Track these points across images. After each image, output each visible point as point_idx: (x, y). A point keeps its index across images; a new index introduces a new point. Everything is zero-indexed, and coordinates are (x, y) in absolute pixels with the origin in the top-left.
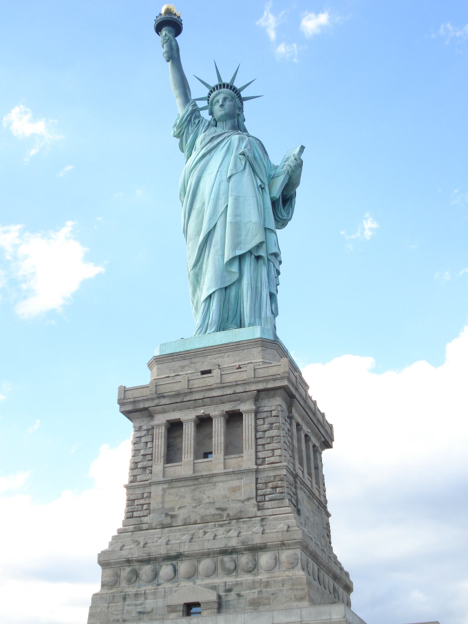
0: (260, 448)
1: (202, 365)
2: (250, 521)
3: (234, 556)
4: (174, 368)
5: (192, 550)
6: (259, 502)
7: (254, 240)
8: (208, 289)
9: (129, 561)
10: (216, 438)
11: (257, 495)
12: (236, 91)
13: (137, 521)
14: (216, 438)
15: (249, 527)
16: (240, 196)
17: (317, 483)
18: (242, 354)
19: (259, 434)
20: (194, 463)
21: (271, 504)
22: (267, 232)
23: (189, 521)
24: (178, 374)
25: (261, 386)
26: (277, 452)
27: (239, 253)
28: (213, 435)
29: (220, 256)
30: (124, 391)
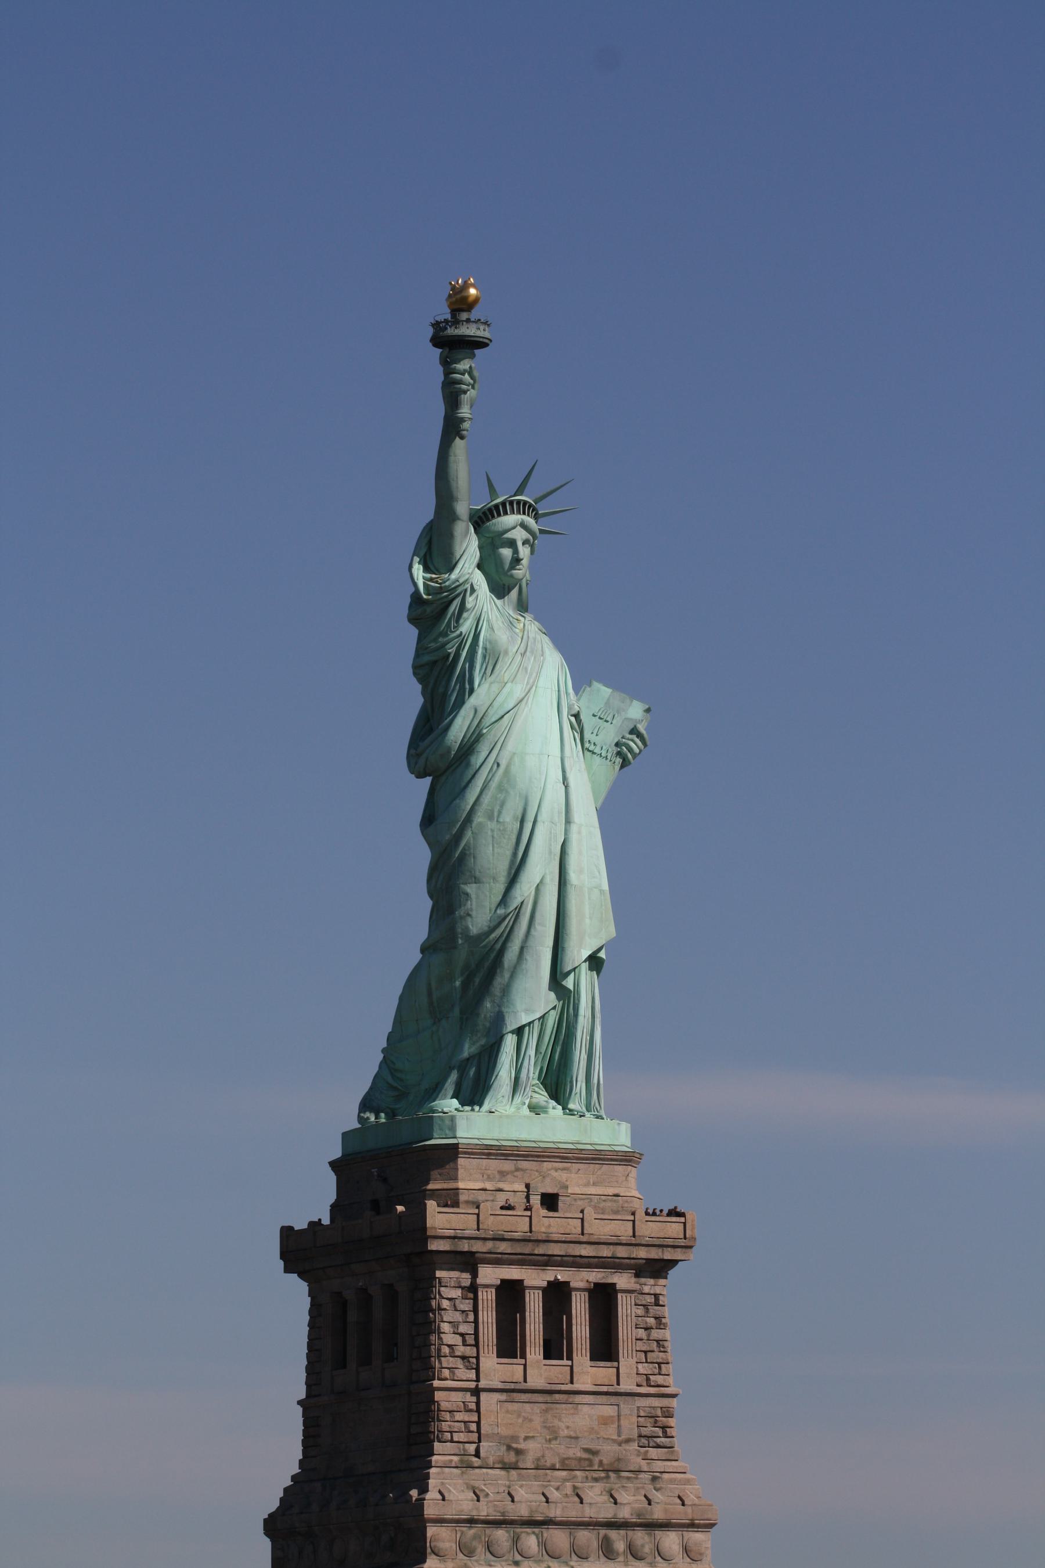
1: (542, 1181)
2: (637, 1478)
3: (622, 1532)
5: (567, 1516)
6: (641, 1447)
9: (471, 1521)
10: (579, 1327)
11: (640, 1436)
13: (459, 1448)
14: (579, 1327)
15: (638, 1488)
18: (599, 1173)
21: (657, 1453)
23: (544, 1463)
24: (501, 1185)
25: (654, 1254)
27: (586, 953)
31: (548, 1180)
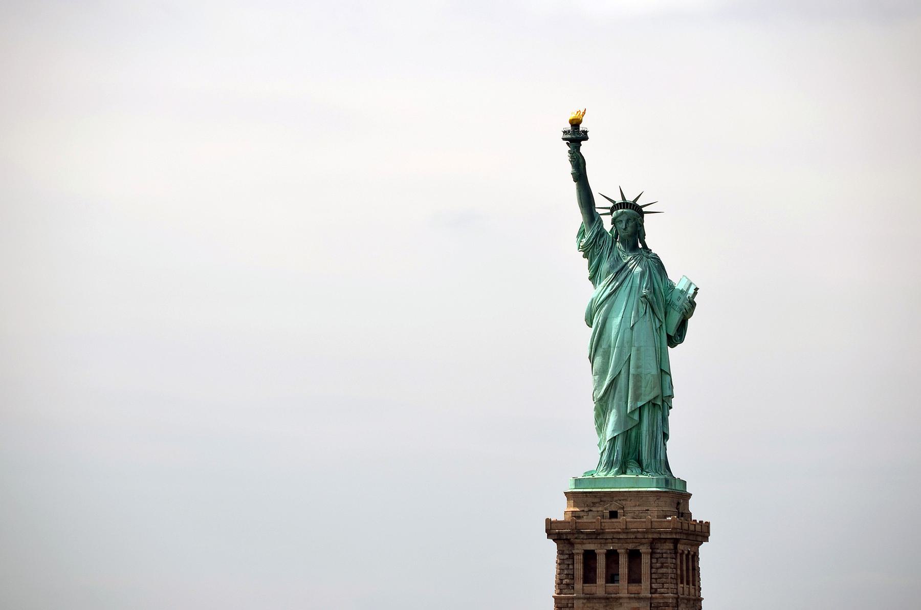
0: (654, 581)
4: (588, 503)
7: (652, 393)
8: (614, 431)
12: (639, 208)
16: (640, 347)
17: (694, 585)
18: (642, 500)
19: (654, 570)
20: (605, 586)
22: (663, 373)
25: (656, 536)
26: (666, 585)
27: (640, 404)
28: (620, 567)
29: (624, 403)
30: (549, 522)
31: (613, 505)
